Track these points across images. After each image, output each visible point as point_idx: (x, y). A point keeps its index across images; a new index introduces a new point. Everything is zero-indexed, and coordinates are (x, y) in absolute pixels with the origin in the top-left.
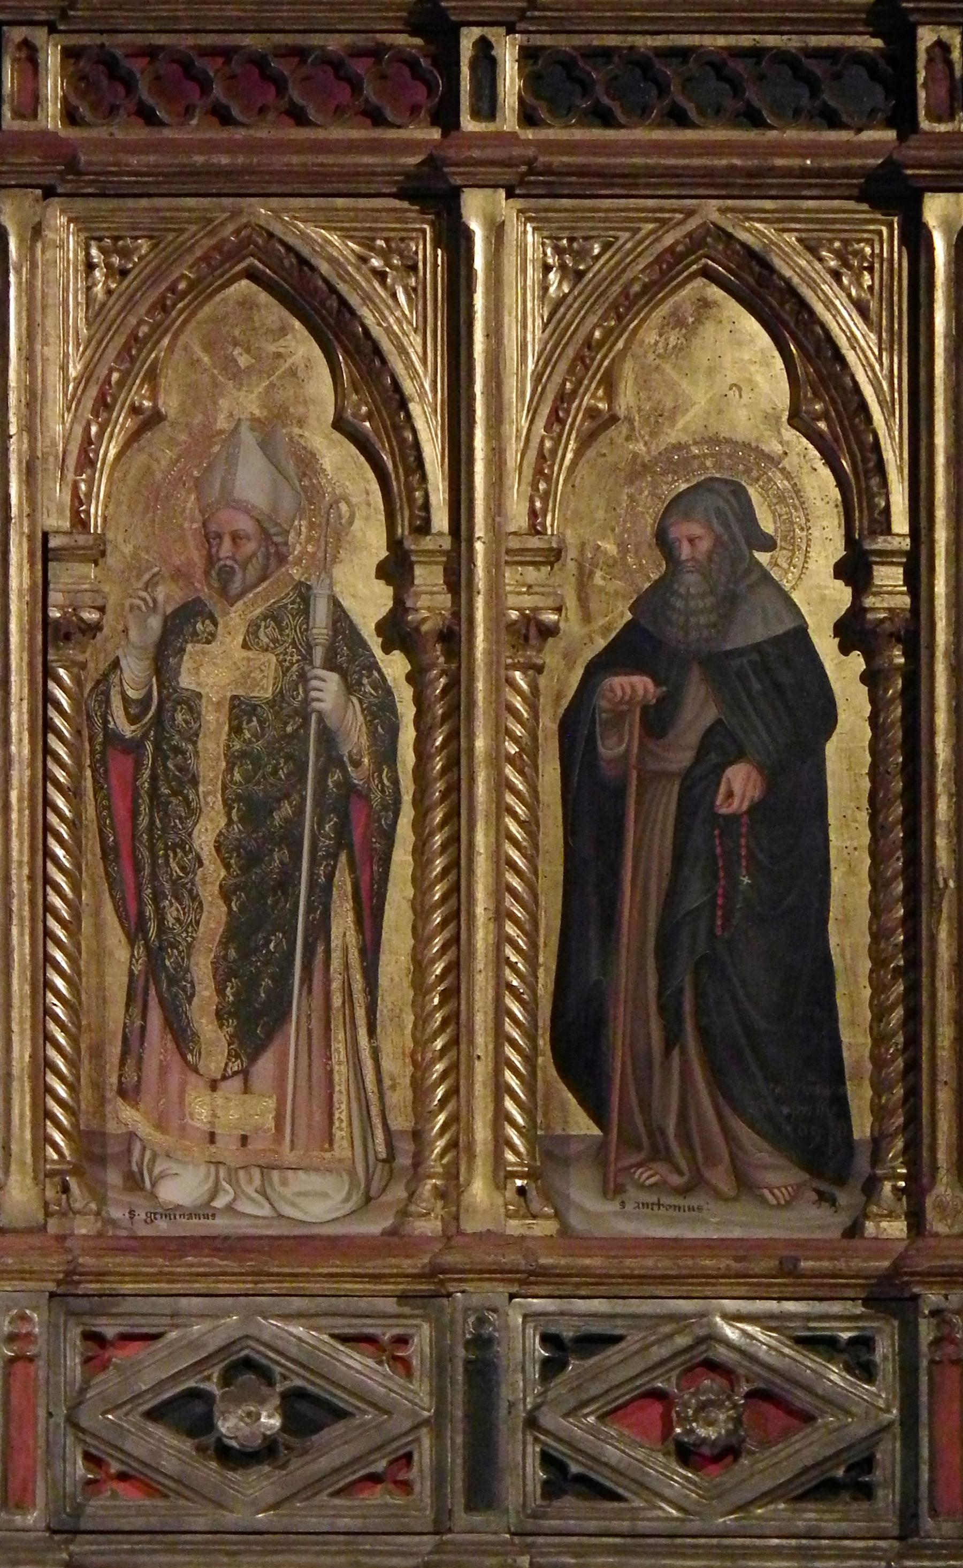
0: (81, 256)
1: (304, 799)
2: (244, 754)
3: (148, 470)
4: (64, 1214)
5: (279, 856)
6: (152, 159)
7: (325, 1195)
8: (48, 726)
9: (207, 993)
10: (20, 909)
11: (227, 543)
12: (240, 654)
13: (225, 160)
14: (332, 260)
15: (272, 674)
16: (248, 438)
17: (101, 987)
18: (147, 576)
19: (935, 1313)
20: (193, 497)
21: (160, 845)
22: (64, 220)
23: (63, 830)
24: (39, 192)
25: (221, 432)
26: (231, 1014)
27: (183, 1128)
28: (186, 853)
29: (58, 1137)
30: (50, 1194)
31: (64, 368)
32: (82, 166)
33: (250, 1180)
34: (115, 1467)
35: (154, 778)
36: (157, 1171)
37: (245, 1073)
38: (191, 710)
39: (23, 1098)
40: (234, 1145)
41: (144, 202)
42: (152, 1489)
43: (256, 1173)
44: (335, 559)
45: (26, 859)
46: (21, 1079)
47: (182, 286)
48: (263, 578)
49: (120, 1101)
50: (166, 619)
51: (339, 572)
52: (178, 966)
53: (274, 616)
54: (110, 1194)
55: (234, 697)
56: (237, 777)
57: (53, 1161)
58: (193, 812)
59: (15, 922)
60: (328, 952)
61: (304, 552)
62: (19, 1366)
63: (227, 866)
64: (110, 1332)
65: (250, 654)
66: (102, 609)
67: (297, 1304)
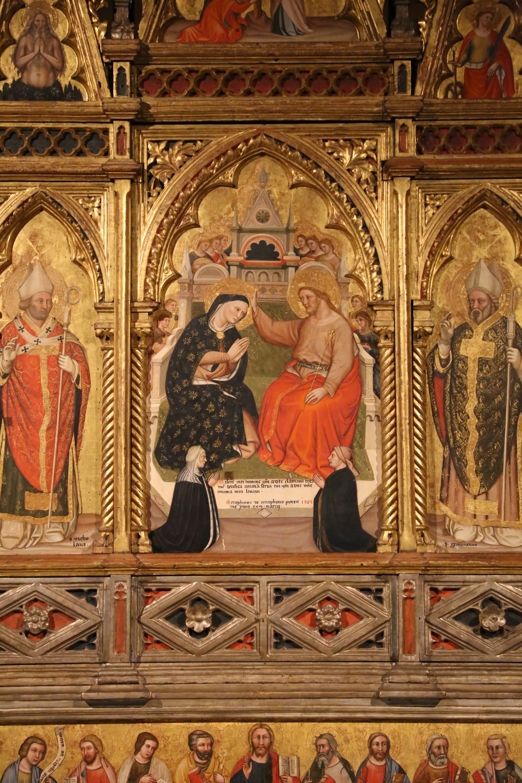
0: (423, 201)
1: (506, 394)
2: (483, 378)
3: (447, 277)
4: (423, 545)
5: (498, 414)
6: (450, 166)
7: (517, 537)
8: (414, 369)
9: (472, 464)
10: (406, 435)
11: (476, 303)
12: (481, 342)
13: (476, 166)
14: (514, 201)
15: (493, 350)
16: (483, 265)
17: (433, 462)
18: (447, 315)
20: (464, 287)
21: (454, 411)
22: (417, 188)
23: (419, 406)
24: (409, 178)
25: (475, 263)
26: (481, 472)
27: (464, 512)
28: (463, 414)
29: (419, 517)
30: (418, 537)
31: (417, 241)
32: (425, 169)
33: (489, 531)
34: (443, 637)
35: (451, 387)
36: (455, 529)
37: (486, 493)
38: (464, 362)
39: (408, 503)
40: (483, 519)
41: (446, 182)
42: (457, 646)
43: (491, 529)
44: (516, 308)
45: (407, 417)
46: (407, 496)
47: (459, 211)
48: (490, 315)
49: (441, 503)
50: (455, 330)
51: (517, 312)
52: (461, 454)
53: (494, 329)
54: (438, 537)
55: (480, 358)
56: (481, 386)
57: (418, 526)
58: (465, 399)
59: (404, 439)
60: (516, 449)
61: (504, 306)
62: (408, 601)
63: (479, 419)
64: (440, 588)
65: (485, 342)
66: (432, 327)
67: (509, 578)
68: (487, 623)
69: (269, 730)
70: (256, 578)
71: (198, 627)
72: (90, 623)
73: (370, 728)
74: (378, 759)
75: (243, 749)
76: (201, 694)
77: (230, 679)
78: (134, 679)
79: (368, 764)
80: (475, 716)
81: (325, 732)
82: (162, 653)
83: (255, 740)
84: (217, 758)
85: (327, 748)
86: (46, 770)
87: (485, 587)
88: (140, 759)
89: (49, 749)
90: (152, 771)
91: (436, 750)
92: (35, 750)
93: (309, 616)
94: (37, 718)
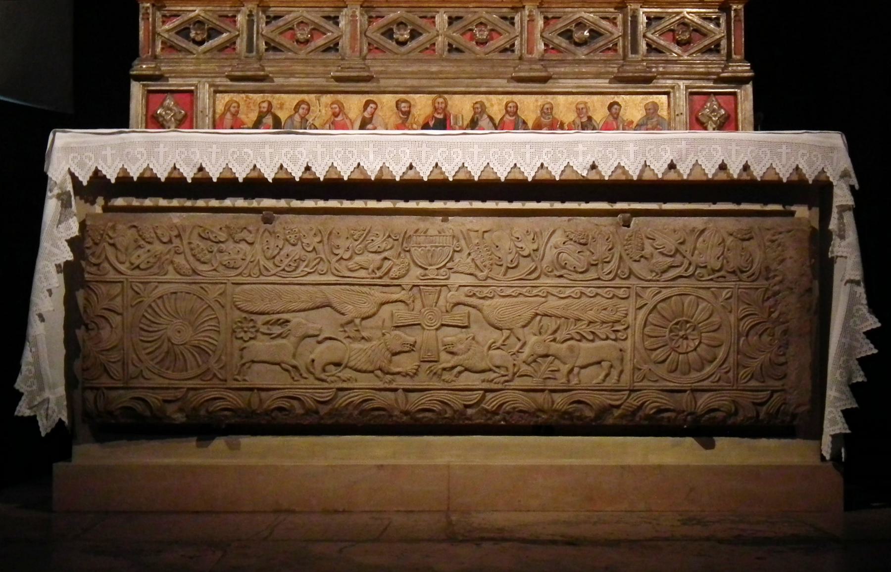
19: (735, 10)
34: (551, 46)
42: (560, 51)
64: (550, 16)
67: (591, 10)
68: (577, 36)
69: (445, 99)
70: (438, 9)
71: (401, 39)
72: (336, 35)
73: (506, 98)
74: (511, 116)
75: (429, 110)
76: (405, 76)
77: (421, 69)
78: (363, 66)
79: (505, 119)
80: (570, 90)
81: (479, 100)
82: (379, 55)
83: (437, 105)
84: (414, 115)
85: (480, 110)
86: (310, 121)
87: (577, 16)
88: (367, 115)
89: (312, 108)
90: (374, 121)
91: (545, 111)
92: (303, 109)
93: (469, 34)
94: (304, 89)
